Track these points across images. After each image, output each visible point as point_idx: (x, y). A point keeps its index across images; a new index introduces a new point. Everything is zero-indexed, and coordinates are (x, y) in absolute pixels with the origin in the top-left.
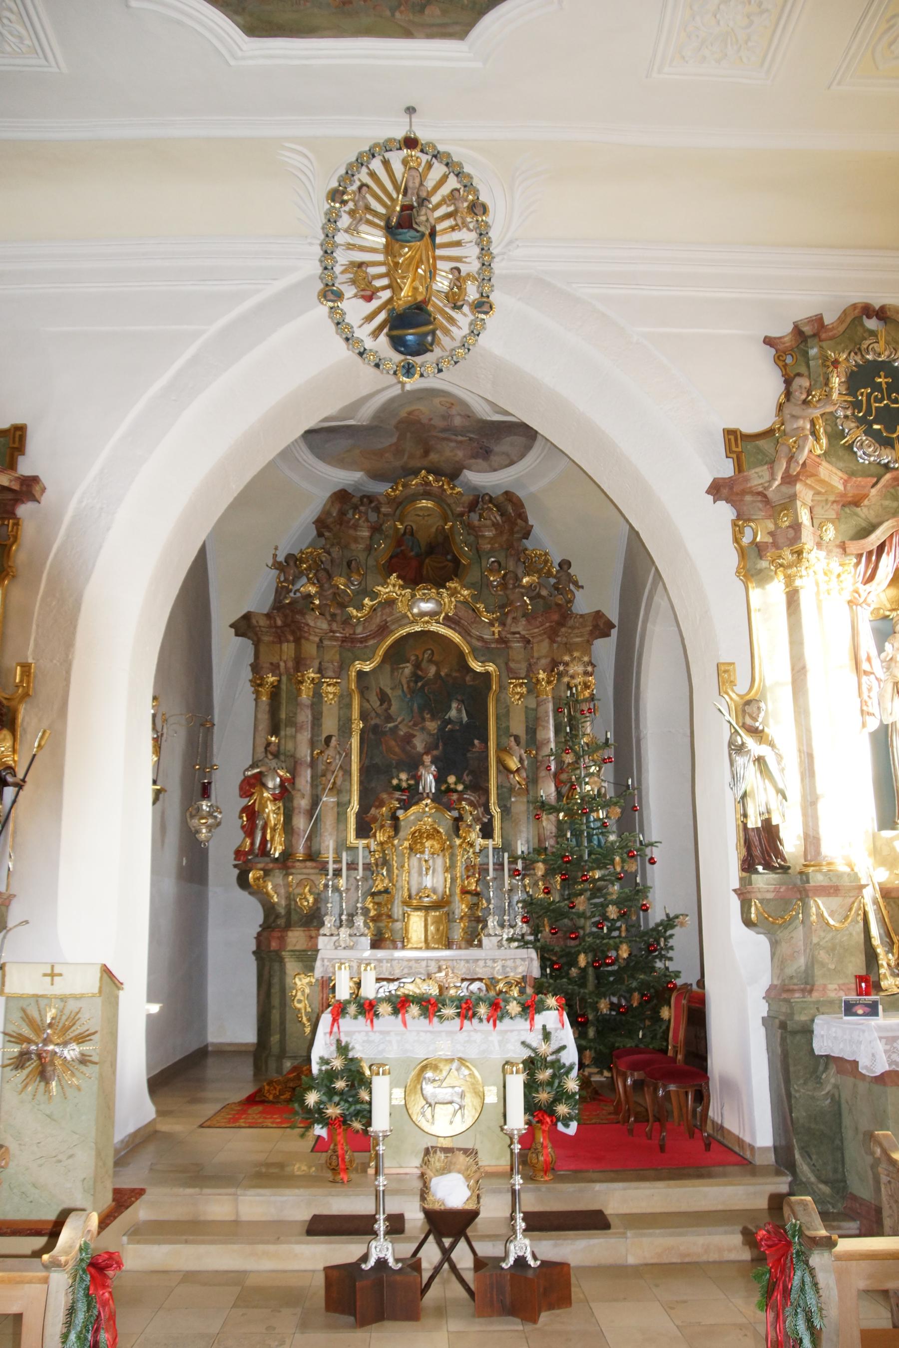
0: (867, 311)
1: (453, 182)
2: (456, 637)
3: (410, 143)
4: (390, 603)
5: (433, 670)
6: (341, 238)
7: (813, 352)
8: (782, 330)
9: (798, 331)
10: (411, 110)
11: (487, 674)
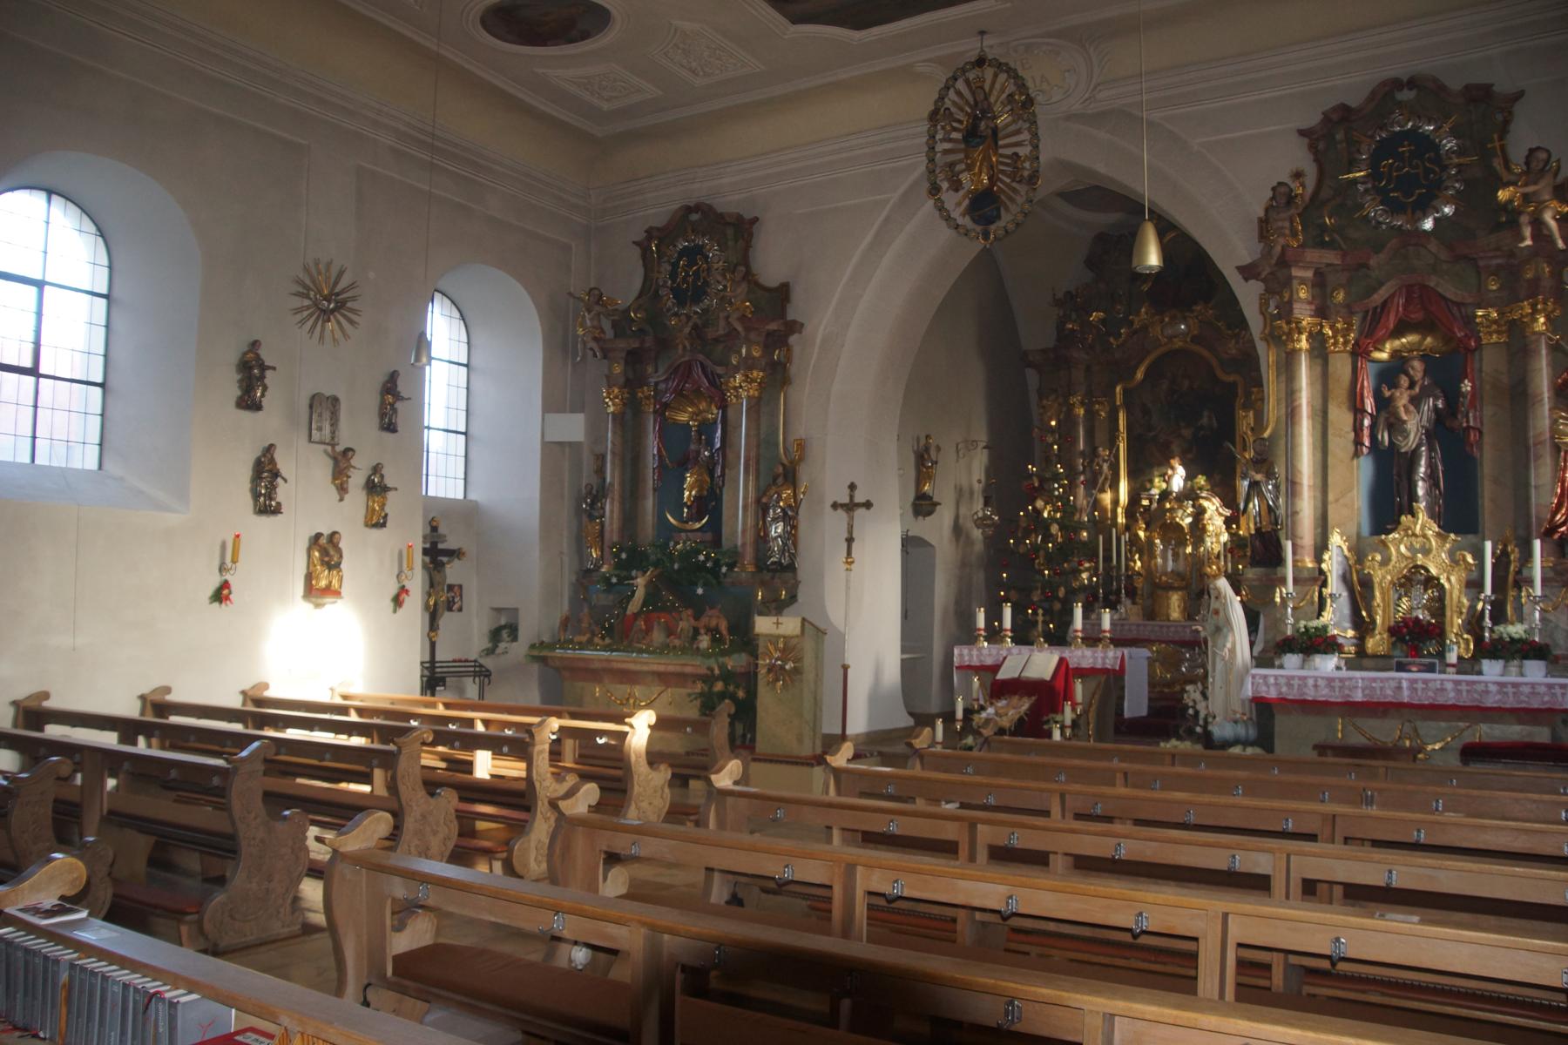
0: (1396, 84)
1: (1011, 88)
2: (1205, 353)
3: (981, 62)
4: (1145, 328)
5: (1186, 383)
6: (940, 147)
7: (1339, 136)
8: (1313, 119)
9: (1327, 118)
10: (982, 33)
11: (1234, 384)
